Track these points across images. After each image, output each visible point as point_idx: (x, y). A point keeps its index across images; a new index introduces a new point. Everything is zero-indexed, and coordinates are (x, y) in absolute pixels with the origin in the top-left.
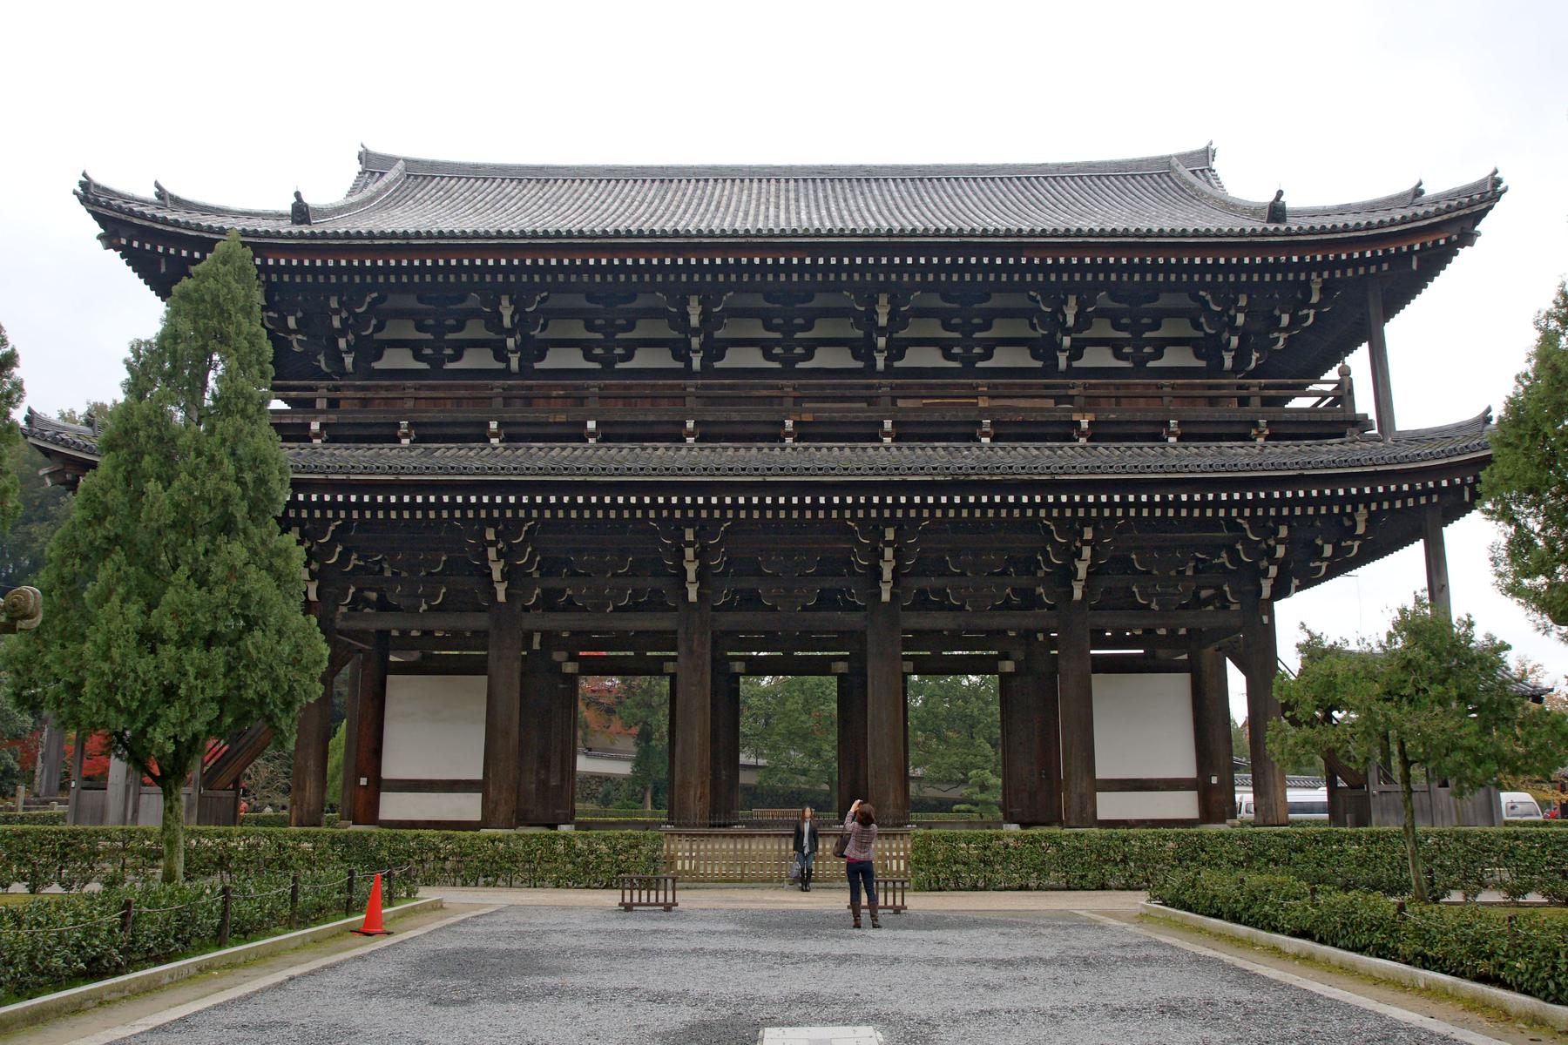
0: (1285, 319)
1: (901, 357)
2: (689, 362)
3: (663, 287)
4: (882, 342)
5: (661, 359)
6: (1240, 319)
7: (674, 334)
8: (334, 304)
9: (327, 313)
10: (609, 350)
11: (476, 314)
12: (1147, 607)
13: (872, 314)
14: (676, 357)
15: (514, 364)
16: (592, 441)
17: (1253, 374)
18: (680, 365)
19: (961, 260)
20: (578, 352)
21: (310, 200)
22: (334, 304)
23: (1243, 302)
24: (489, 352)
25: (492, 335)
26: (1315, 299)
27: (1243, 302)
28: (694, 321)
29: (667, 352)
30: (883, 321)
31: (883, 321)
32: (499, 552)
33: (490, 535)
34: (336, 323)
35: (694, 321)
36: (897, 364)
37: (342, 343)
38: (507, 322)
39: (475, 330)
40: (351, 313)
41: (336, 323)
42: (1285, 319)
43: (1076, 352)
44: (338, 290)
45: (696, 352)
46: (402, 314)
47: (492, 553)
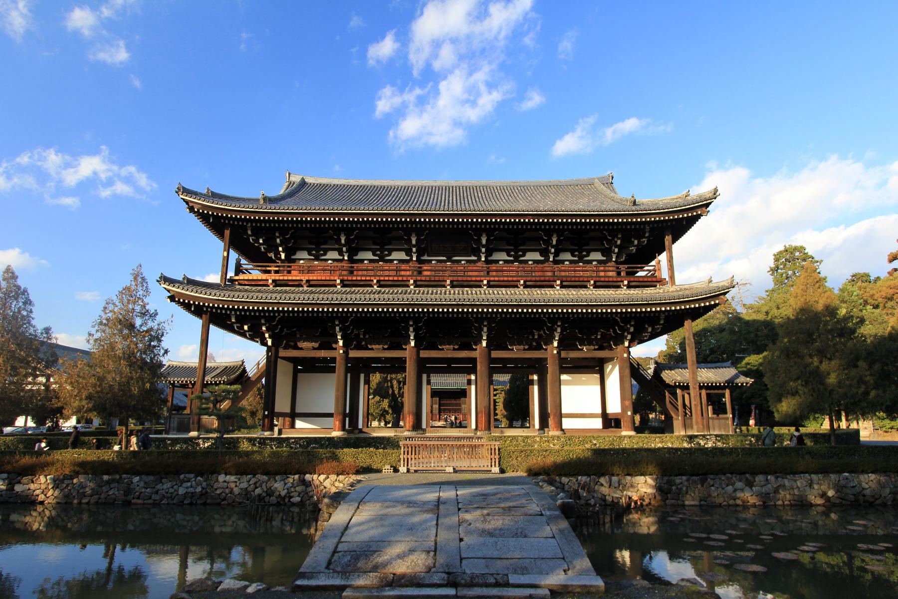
0: (636, 242)
1: (491, 255)
2: (412, 257)
3: (402, 229)
4: (483, 250)
5: (402, 256)
6: (619, 242)
7: (406, 246)
8: (277, 234)
10: (382, 252)
11: (331, 238)
12: (582, 350)
13: (480, 240)
14: (407, 255)
17: (622, 263)
22: (277, 234)
23: (620, 236)
24: (336, 253)
25: (337, 246)
26: (647, 235)
27: (620, 236)
28: (414, 242)
30: (484, 242)
31: (484, 242)
34: (278, 241)
35: (414, 242)
36: (490, 258)
37: (280, 249)
38: (343, 242)
40: (284, 238)
41: (278, 241)
42: (636, 242)
43: (556, 254)
44: (279, 229)
47: (337, 329)
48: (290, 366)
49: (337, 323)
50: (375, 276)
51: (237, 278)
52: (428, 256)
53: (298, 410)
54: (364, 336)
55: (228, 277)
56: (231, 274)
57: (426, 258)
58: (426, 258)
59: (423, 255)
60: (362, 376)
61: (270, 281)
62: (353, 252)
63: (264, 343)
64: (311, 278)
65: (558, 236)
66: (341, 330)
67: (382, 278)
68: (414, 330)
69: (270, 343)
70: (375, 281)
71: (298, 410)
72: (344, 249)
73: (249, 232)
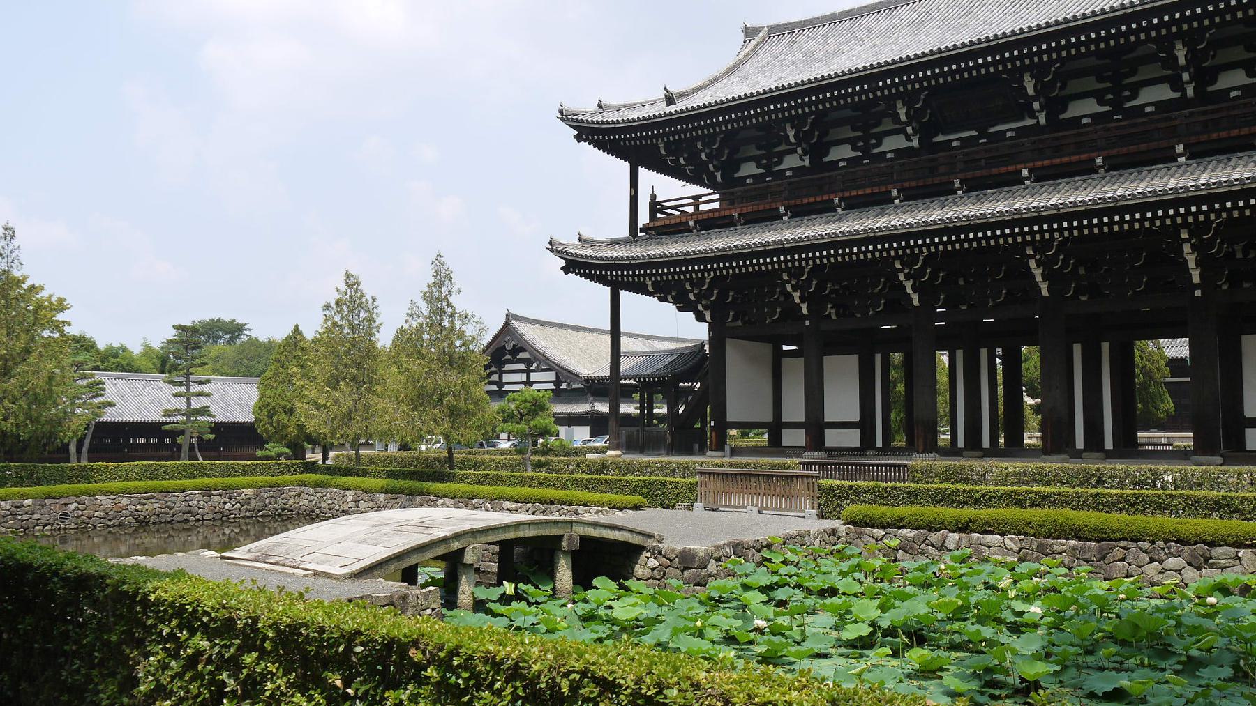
9: (699, 152)
11: (886, 115)
15: (1190, 92)
16: (1028, 182)
18: (1178, 95)
19: (1155, 21)
20: (1093, 101)
21: (675, 89)
29: (1166, 86)
32: (793, 286)
33: (1184, 235)
34: (703, 156)
39: (887, 125)
41: (703, 156)
45: (1188, 83)
46: (840, 123)
47: (1187, 248)
48: (766, 349)
49: (1184, 235)
50: (835, 192)
51: (656, 224)
52: (945, 133)
53: (784, 419)
54: (1245, 253)
55: (640, 226)
56: (644, 218)
57: (940, 138)
58: (940, 138)
59: (936, 135)
60: (878, 357)
61: (691, 223)
62: (1204, 77)
63: (700, 318)
64: (745, 210)
65: (1037, 77)
66: (794, 288)
67: (847, 194)
68: (1194, 248)
69: (708, 318)
70: (836, 200)
71: (784, 419)
72: (1186, 77)
73: (663, 152)
